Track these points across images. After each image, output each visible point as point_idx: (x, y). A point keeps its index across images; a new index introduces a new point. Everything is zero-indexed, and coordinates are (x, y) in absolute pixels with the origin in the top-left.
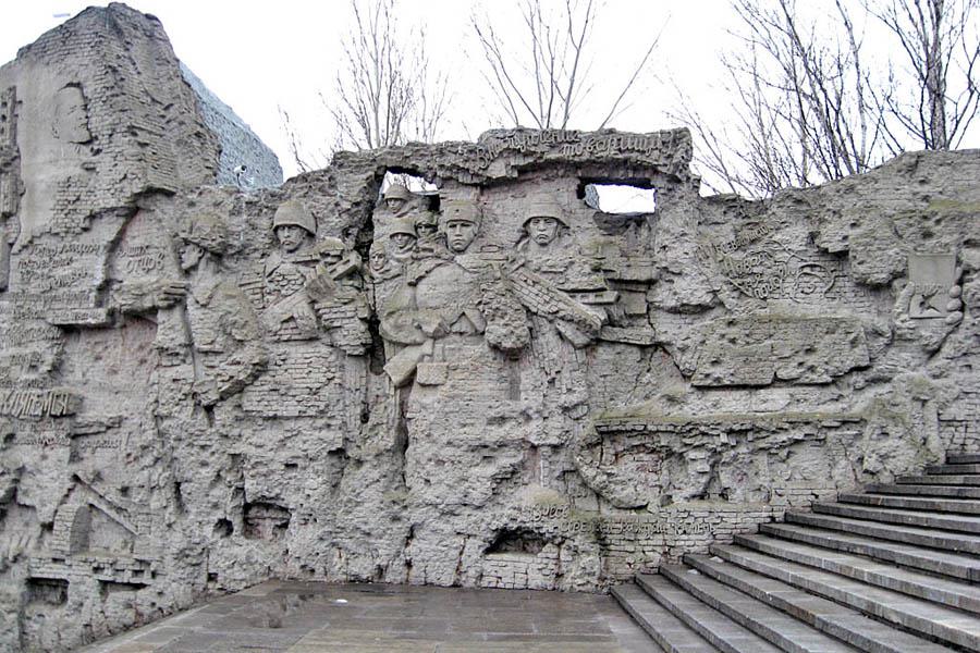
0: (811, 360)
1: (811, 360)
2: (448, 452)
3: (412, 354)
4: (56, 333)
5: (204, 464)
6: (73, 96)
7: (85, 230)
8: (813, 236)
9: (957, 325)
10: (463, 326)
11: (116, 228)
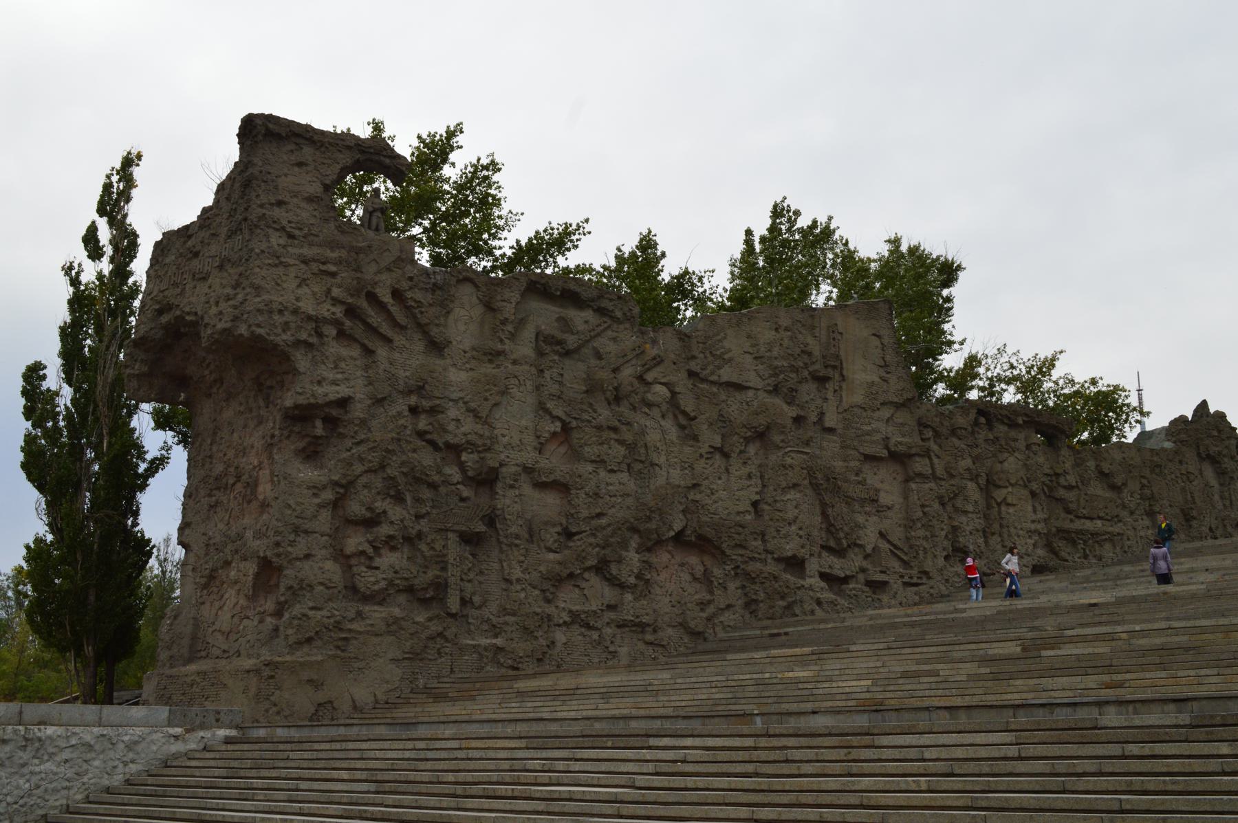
0: (1107, 511)
1: (1107, 511)
2: (1021, 532)
3: (1004, 491)
4: (862, 458)
5: (942, 529)
6: (875, 342)
7: (878, 409)
8: (1097, 466)
9: (1139, 504)
10: (1021, 482)
11: (892, 411)
